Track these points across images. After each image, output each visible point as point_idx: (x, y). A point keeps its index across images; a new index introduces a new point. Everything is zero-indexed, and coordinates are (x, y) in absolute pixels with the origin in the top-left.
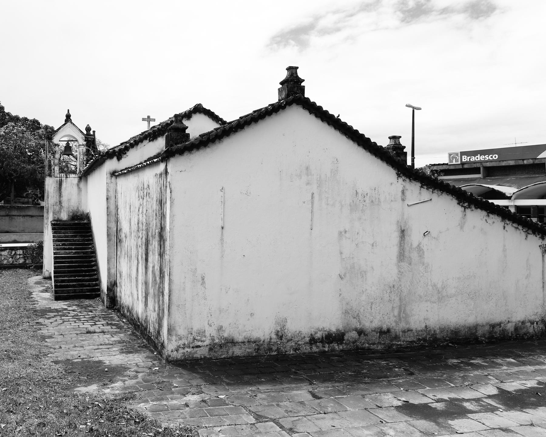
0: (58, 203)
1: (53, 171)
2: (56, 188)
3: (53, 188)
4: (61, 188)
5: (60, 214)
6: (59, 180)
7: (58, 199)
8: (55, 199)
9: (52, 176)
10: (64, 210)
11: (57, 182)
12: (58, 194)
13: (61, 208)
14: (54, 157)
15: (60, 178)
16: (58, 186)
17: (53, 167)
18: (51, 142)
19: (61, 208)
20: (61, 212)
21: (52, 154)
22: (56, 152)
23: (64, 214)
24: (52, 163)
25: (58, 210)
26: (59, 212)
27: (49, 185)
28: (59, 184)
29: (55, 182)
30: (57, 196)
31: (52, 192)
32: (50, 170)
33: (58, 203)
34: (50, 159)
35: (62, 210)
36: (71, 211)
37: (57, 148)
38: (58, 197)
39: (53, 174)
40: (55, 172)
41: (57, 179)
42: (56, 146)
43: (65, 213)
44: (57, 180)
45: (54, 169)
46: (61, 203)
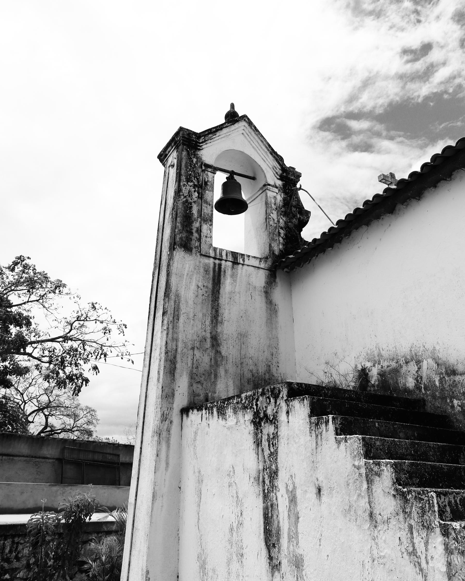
0: (208, 344)
1: (196, 235)
2: (204, 290)
3: (193, 287)
4: (218, 292)
5: (214, 383)
6: (212, 266)
7: (208, 329)
8: (200, 327)
9: (194, 250)
10: (226, 371)
11: (206, 271)
12: (207, 309)
13: (216, 362)
14: (201, 197)
15: (217, 262)
16: (210, 286)
17: (196, 225)
18: (196, 156)
19: (216, 362)
20: (216, 376)
21: (195, 185)
22: (206, 183)
23: (227, 387)
24: (195, 210)
25: (208, 368)
26: (209, 375)
27: (181, 276)
28: (214, 280)
29: (202, 270)
30: (204, 315)
31: (191, 303)
32: (187, 231)
33: (209, 340)
34: (190, 200)
35: (221, 371)
36: (249, 375)
37: (209, 174)
38: (208, 322)
39: (197, 244)
40: (203, 239)
41: (206, 261)
42: (209, 170)
43: (231, 383)
44: (206, 265)
45: (199, 231)
46: (218, 345)
